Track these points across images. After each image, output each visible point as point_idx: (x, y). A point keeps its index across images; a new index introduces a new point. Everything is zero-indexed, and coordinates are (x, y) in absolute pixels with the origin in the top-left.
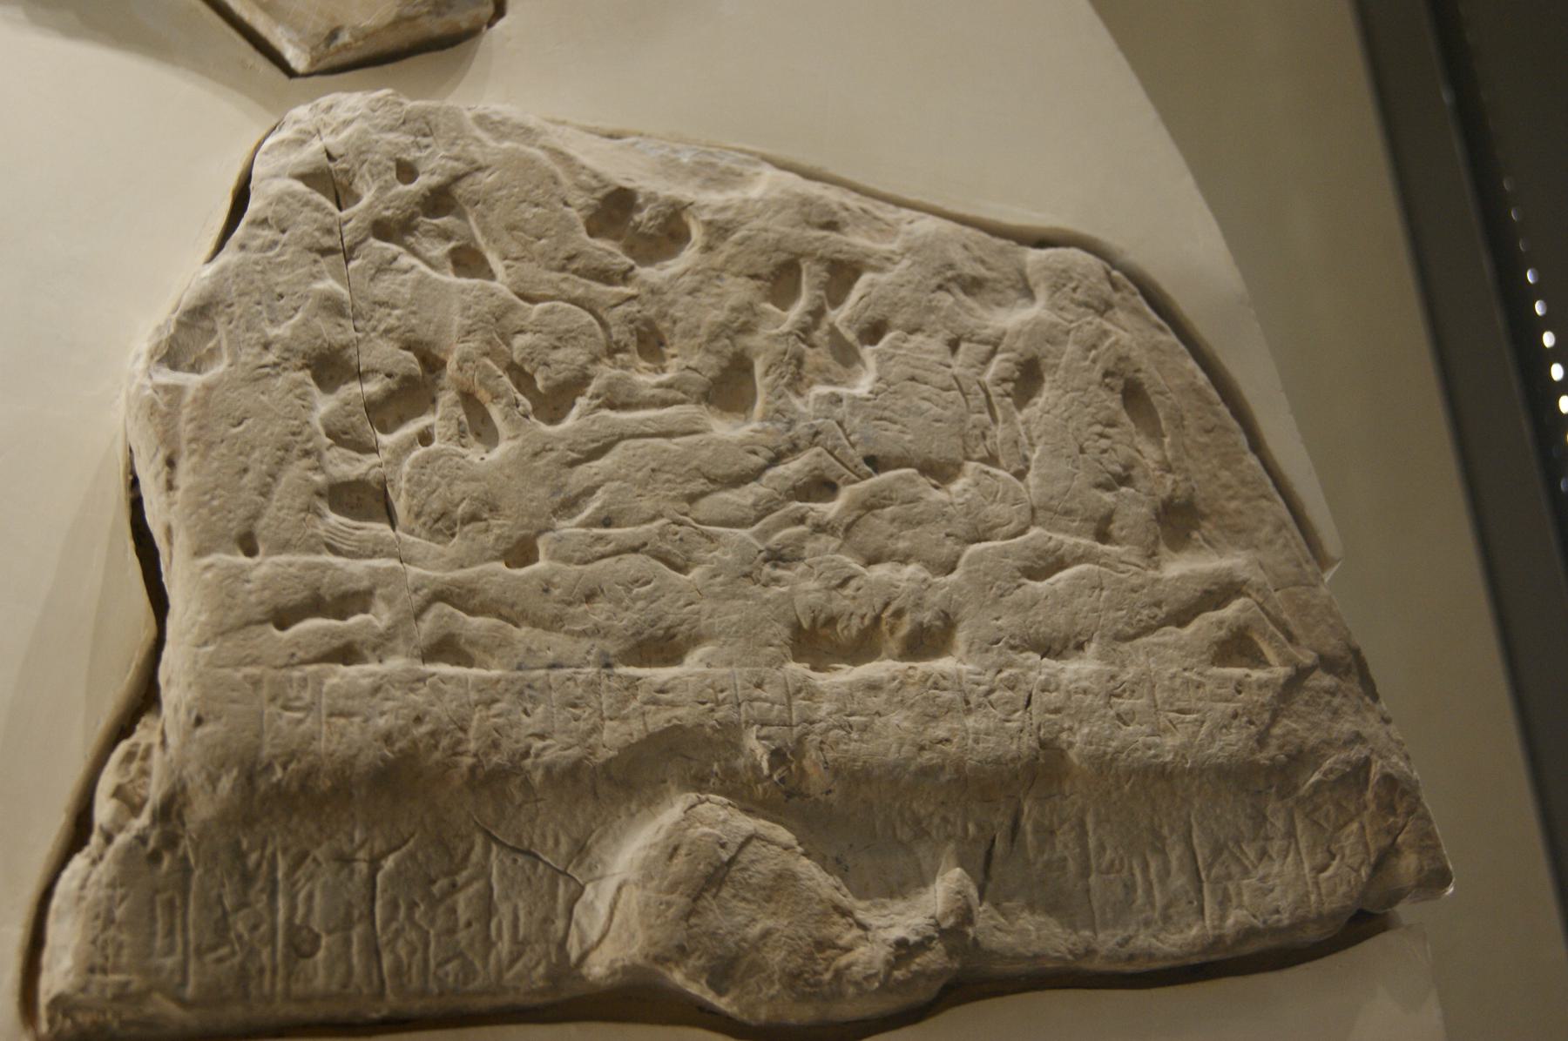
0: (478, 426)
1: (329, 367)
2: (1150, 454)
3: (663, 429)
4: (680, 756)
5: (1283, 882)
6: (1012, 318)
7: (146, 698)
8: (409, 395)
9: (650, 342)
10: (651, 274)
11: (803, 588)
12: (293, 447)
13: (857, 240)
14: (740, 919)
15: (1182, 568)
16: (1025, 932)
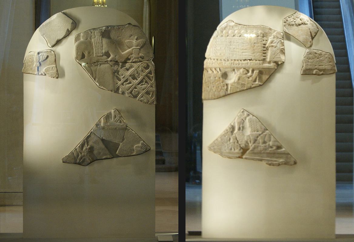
0: (311, 60)
1: (308, 58)
2: (330, 60)
3: (316, 60)
4: (316, 69)
5: (331, 72)
6: (326, 56)
7: (303, 66)
8: (310, 59)
9: (316, 57)
10: (316, 55)
11: (319, 64)
12: (307, 61)
13: (322, 54)
14: (317, 73)
15: (330, 63)
16: (324, 73)
